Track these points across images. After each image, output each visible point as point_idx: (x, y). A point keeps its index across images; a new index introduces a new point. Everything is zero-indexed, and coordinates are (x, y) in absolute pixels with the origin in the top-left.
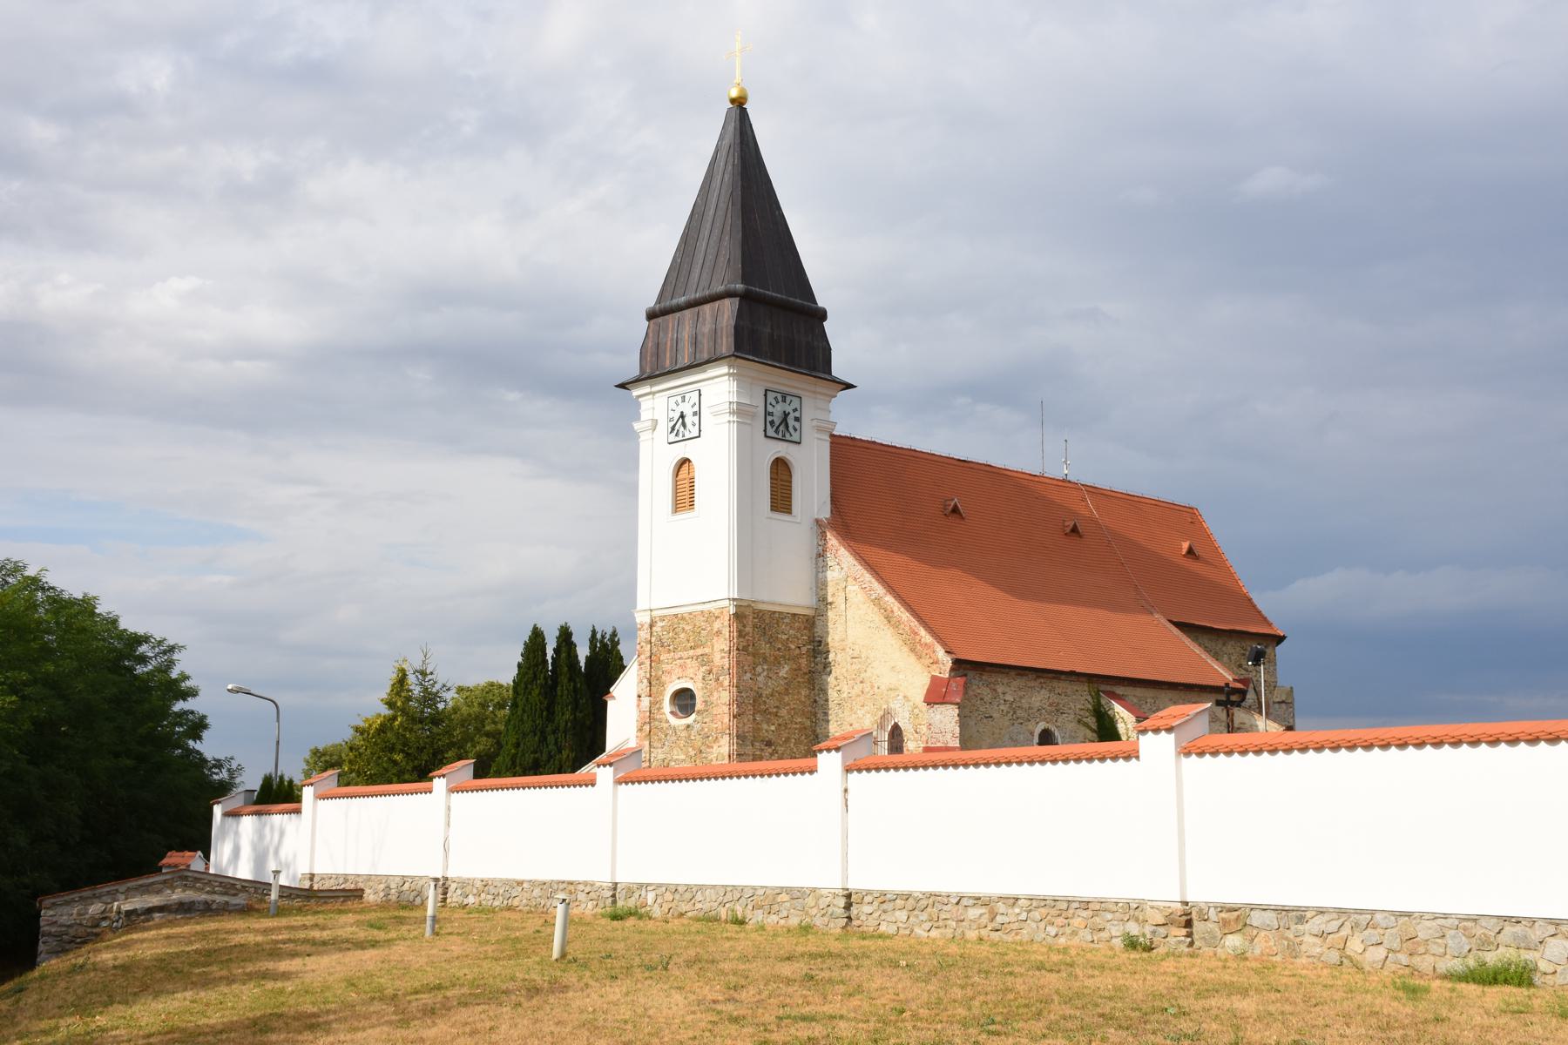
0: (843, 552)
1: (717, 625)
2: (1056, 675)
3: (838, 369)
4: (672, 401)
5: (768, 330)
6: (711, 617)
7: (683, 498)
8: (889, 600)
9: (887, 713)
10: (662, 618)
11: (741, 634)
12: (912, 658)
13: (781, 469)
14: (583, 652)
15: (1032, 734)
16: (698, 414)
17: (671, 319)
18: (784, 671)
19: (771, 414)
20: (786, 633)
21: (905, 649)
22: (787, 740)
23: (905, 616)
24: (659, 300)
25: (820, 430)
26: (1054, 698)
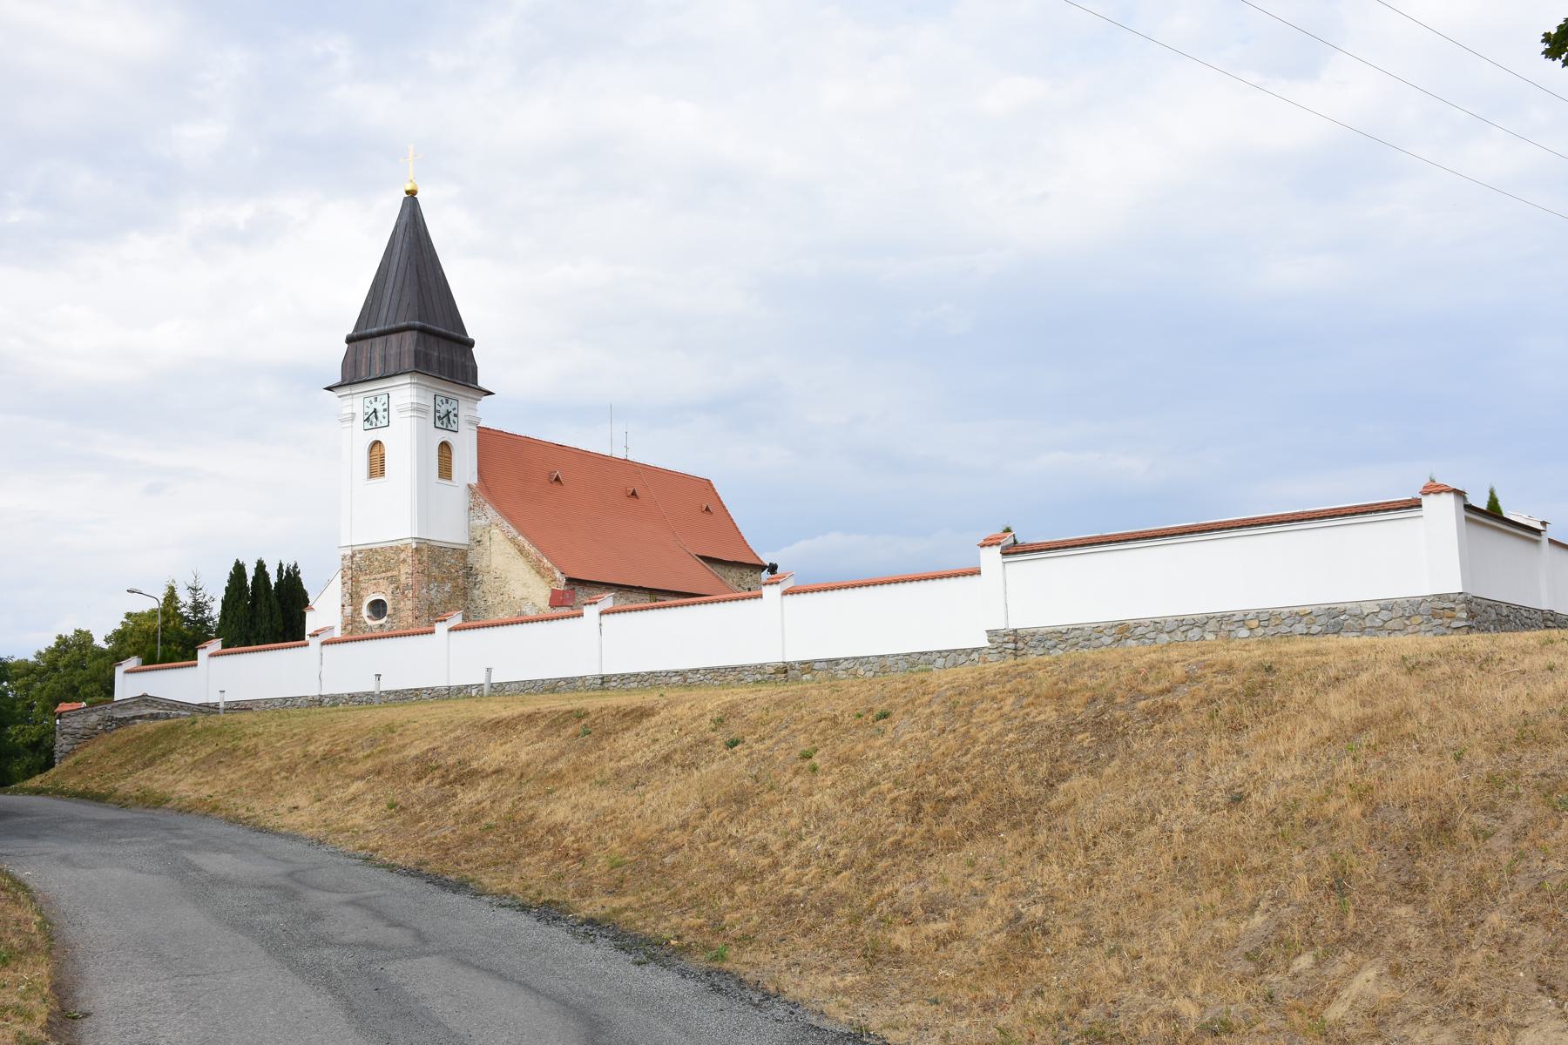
1: (402, 556)
3: (482, 383)
6: (398, 550)
13: (445, 447)
14: (273, 580)
17: (365, 344)
20: (449, 561)
24: (357, 327)
25: (470, 423)
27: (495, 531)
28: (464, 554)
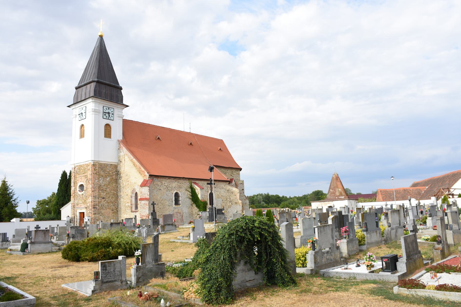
0: (124, 148)
1: (89, 167)
2: (180, 178)
3: (125, 102)
5: (104, 91)
6: (88, 165)
7: (82, 135)
8: (134, 160)
9: (134, 190)
10: (77, 166)
11: (95, 170)
12: (140, 175)
16: (85, 112)
17: (80, 89)
18: (108, 179)
22: (109, 197)
23: (138, 164)
25: (119, 117)
26: (179, 184)
27: (126, 157)
28: (116, 167)
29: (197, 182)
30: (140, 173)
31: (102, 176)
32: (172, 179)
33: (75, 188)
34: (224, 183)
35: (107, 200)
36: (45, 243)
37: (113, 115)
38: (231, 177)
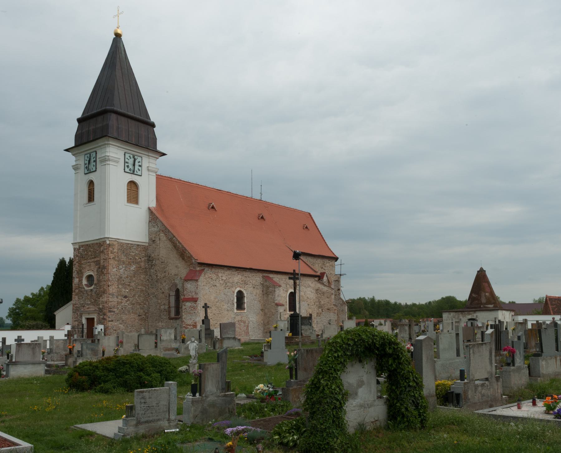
3: (160, 148)
4: (86, 156)
10: (82, 246)
15: (234, 292)
19: (127, 163)
21: (181, 259)
22: (134, 296)
26: (244, 278)
28: (145, 248)
29: (271, 276)
30: (183, 259)
31: (124, 263)
32: (234, 270)
33: (81, 281)
34: (312, 279)
35: (131, 299)
36: (33, 364)
37: (140, 168)
38: (323, 271)
